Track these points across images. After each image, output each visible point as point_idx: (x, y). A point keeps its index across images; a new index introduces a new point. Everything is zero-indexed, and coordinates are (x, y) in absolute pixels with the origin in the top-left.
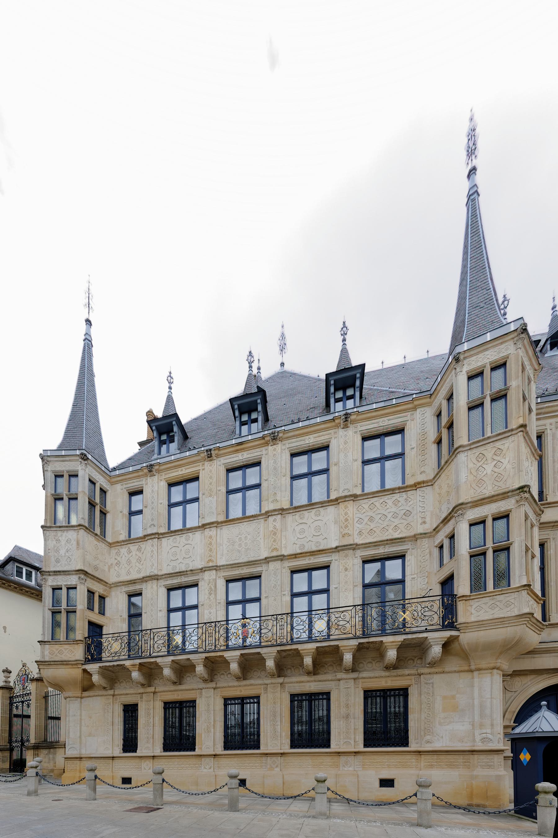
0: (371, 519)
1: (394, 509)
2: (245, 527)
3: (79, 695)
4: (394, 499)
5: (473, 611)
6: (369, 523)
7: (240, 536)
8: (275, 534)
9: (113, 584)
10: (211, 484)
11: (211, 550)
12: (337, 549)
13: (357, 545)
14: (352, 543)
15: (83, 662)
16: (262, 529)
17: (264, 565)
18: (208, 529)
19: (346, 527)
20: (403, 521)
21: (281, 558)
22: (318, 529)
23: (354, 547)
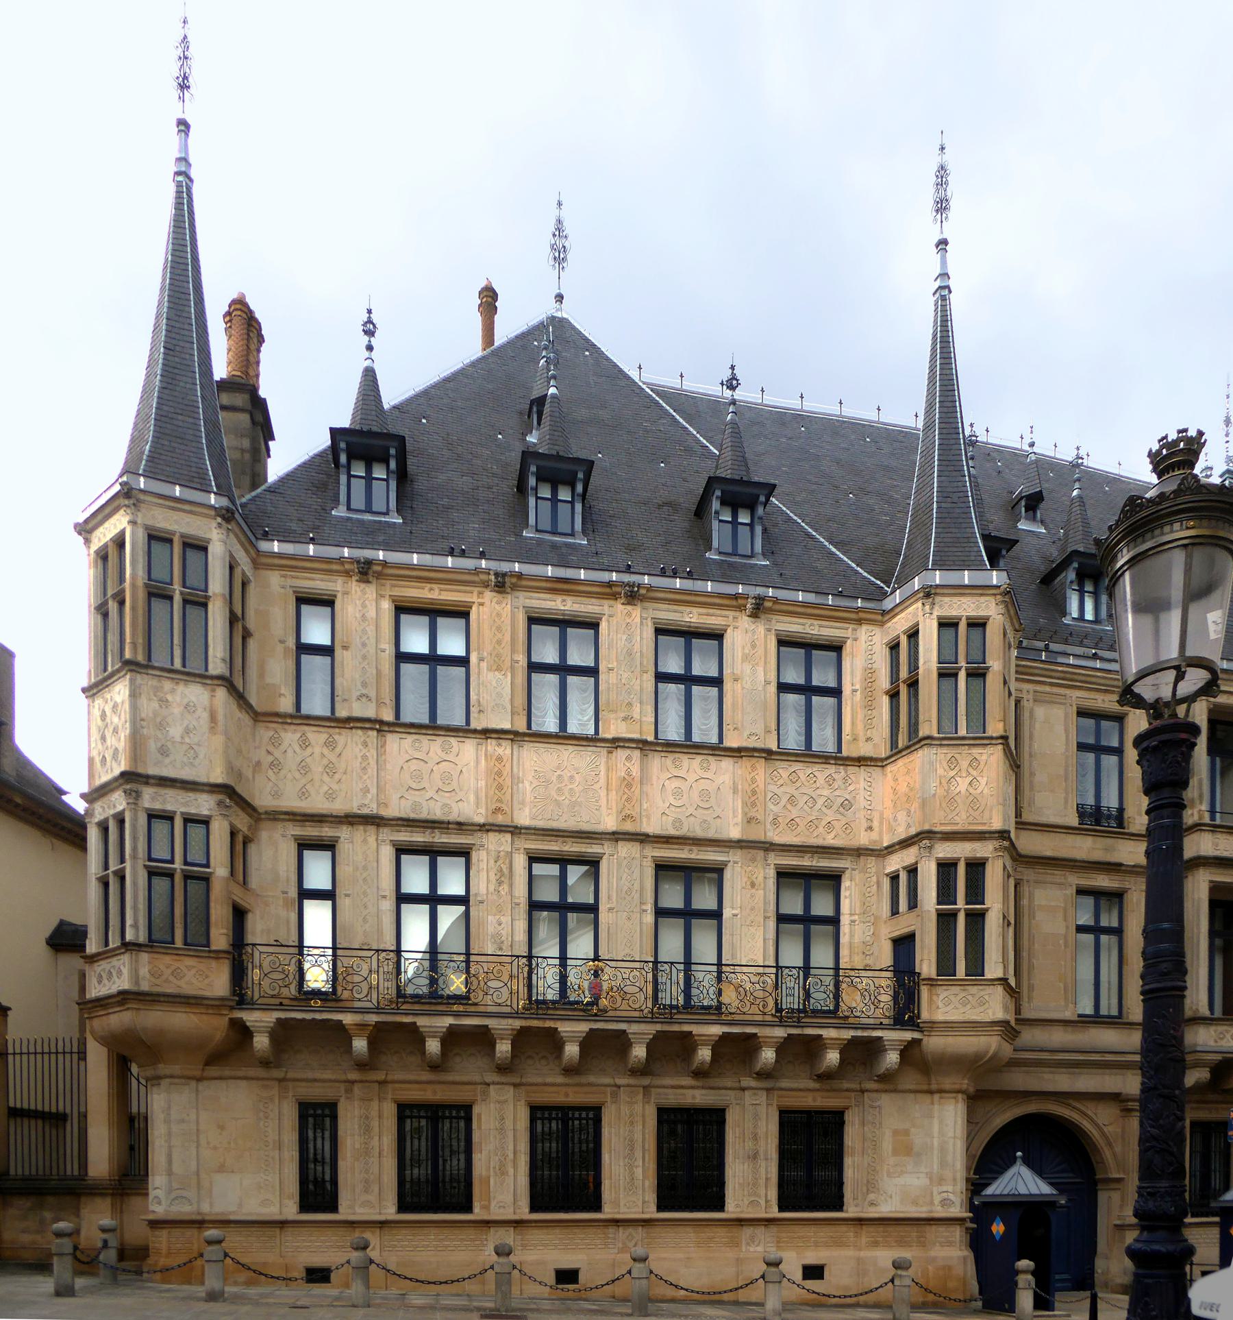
0: (792, 800)
1: (826, 792)
2: (567, 755)
3: (198, 1073)
4: (828, 772)
5: (941, 1005)
6: (789, 806)
7: (559, 772)
8: (629, 786)
9: (266, 813)
10: (499, 642)
11: (500, 787)
12: (740, 844)
13: (772, 844)
14: (763, 839)
15: (233, 1004)
16: (603, 768)
17: (607, 844)
18: (494, 742)
19: (754, 804)
20: (840, 817)
21: (643, 839)
22: (704, 794)
23: (769, 847)
